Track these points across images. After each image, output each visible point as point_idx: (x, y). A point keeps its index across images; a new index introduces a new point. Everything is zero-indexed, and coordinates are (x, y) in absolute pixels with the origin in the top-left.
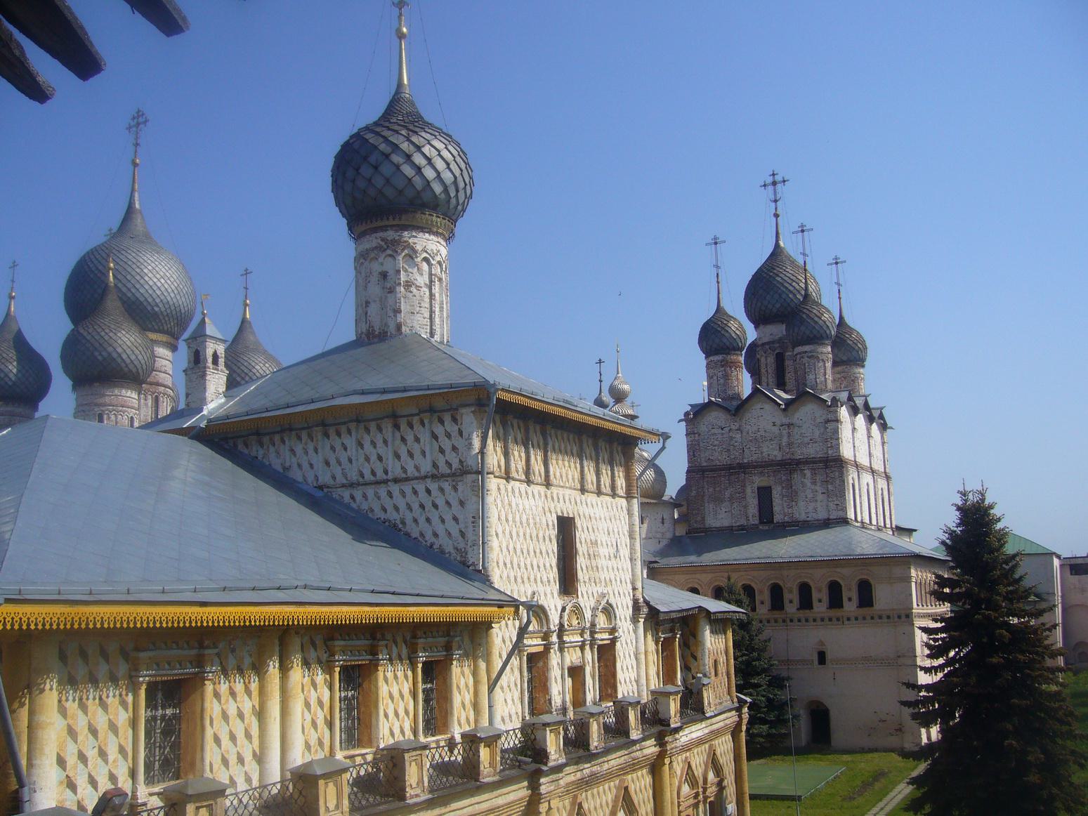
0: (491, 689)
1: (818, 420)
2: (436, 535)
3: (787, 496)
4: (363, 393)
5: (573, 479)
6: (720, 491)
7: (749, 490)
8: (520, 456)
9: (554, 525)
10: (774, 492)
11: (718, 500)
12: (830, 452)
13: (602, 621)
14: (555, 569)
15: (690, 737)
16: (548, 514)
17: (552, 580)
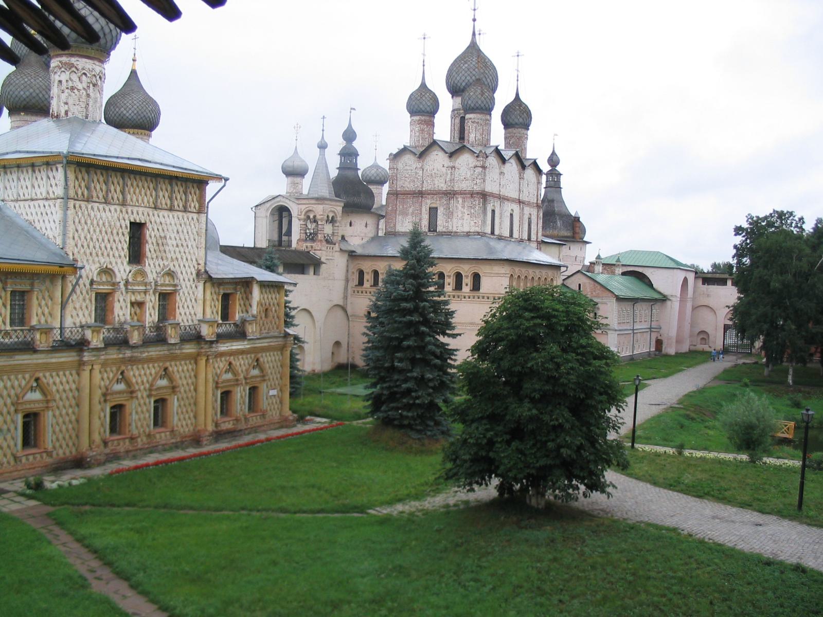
0: (63, 307)
1: (470, 166)
2: (46, 229)
3: (446, 215)
4: (28, 152)
5: (148, 202)
6: (407, 208)
7: (424, 209)
8: (101, 189)
9: (126, 227)
10: (439, 211)
11: (405, 214)
12: (475, 187)
13: (167, 280)
14: (126, 250)
15: (229, 348)
16: (122, 221)
17: (122, 254)
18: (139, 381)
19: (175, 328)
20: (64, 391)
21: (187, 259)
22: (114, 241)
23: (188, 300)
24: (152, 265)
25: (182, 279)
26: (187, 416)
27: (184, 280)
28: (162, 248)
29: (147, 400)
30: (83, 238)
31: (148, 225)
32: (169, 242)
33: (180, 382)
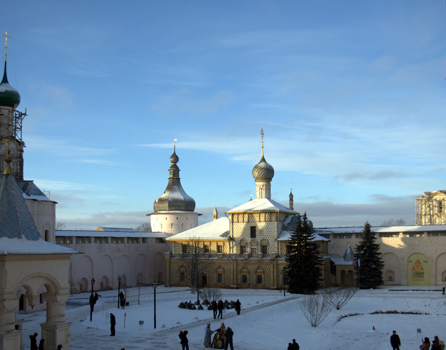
8: (241, 219)
9: (249, 228)
17: (248, 235)
18: (251, 269)
19: (260, 255)
20: (228, 270)
21: (271, 235)
22: (246, 232)
23: (272, 247)
24: (258, 238)
25: (269, 241)
26: (269, 281)
27: (270, 241)
28: (261, 233)
29: (254, 275)
30: (236, 232)
31: (256, 227)
32: (264, 231)
33: (265, 271)
